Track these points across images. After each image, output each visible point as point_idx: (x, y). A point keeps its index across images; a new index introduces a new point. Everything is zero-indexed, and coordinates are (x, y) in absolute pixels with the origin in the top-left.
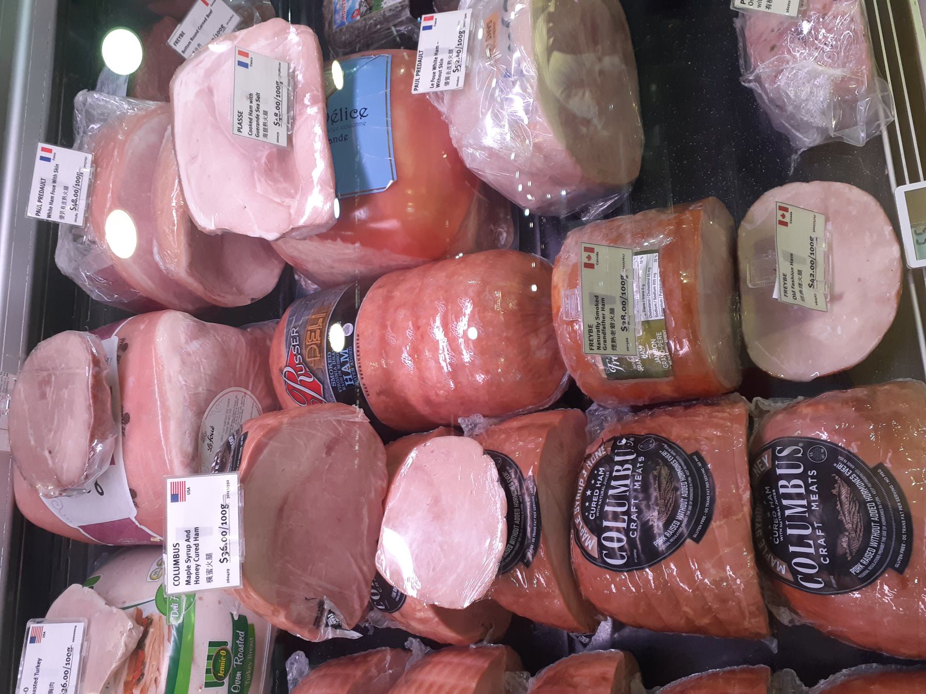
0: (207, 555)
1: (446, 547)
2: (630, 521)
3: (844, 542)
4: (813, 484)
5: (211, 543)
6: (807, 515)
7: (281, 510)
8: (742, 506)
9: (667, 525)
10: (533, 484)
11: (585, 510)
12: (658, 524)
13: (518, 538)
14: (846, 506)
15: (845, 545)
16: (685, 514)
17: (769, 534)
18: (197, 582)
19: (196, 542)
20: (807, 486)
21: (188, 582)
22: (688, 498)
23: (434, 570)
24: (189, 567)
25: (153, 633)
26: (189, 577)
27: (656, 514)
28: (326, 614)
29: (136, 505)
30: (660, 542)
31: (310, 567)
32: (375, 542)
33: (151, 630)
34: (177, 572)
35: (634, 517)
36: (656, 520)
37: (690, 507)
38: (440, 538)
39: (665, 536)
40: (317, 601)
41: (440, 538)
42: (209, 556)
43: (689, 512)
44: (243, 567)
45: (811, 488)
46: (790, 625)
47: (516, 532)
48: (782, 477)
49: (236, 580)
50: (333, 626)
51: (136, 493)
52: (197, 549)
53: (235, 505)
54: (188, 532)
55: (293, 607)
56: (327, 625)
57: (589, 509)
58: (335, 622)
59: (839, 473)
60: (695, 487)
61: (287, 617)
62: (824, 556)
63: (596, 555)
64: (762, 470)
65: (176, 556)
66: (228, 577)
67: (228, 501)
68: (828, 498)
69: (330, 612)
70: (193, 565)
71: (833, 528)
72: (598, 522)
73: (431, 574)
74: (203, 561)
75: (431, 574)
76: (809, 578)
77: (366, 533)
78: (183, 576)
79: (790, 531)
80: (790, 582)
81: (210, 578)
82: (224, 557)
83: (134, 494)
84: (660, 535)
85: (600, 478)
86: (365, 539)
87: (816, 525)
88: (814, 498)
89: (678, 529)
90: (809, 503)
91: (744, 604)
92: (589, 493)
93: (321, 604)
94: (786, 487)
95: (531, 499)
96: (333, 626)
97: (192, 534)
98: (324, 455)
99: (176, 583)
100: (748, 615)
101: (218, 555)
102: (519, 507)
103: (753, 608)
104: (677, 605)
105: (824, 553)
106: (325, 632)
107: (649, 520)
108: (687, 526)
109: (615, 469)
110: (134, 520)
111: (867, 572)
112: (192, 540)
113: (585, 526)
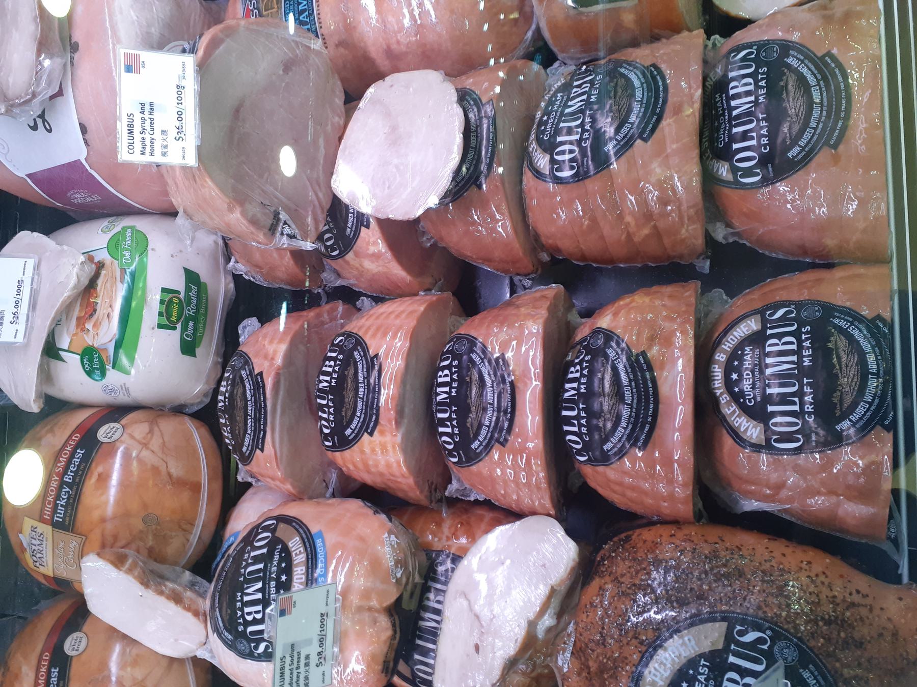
0: (162, 131)
1: (402, 168)
2: (584, 131)
3: (785, 129)
4: (762, 79)
5: (165, 119)
6: (753, 109)
7: (237, 111)
8: (693, 103)
9: (618, 130)
10: (491, 107)
11: (540, 133)
12: (610, 131)
13: (472, 161)
14: (792, 94)
15: (786, 130)
16: (637, 117)
17: (713, 140)
18: (152, 154)
19: (151, 116)
20: (756, 82)
21: (143, 153)
22: (641, 101)
23: (389, 187)
24: (143, 138)
25: (105, 275)
26: (144, 148)
27: (609, 120)
28: (281, 224)
29: (86, 143)
30: (610, 147)
31: (266, 175)
32: (330, 170)
33: (103, 272)
34: (132, 141)
35: (587, 127)
36: (608, 126)
37: (643, 110)
38: (396, 161)
39: (616, 140)
40: (273, 209)
41: (396, 161)
42: (164, 132)
43: (641, 114)
44: (199, 149)
45: (760, 84)
46: (724, 242)
47: (471, 155)
48: (733, 79)
49: (191, 160)
50: (288, 235)
51: (86, 128)
52: (151, 123)
53: (191, 86)
54: (143, 105)
55: (248, 206)
56: (282, 234)
57: (543, 132)
58: (290, 233)
59: (789, 66)
60: (649, 90)
61: (243, 214)
62: (765, 145)
63: (547, 171)
64: (714, 80)
65: (131, 126)
66: (184, 155)
67: (183, 83)
68: (775, 91)
69: (285, 223)
70: (148, 138)
71: (775, 118)
72: (552, 140)
73: (386, 191)
74: (157, 135)
75: (386, 191)
76: (748, 172)
77: (322, 162)
78: (138, 146)
79: (735, 130)
80: (729, 182)
81: (165, 153)
82: (180, 135)
83: (84, 129)
84: (611, 139)
85: (558, 103)
86: (321, 168)
87: (761, 116)
88: (763, 91)
89: (629, 131)
90: (757, 99)
91: (684, 207)
92: (545, 118)
93: (276, 215)
94: (736, 88)
95: (489, 121)
96: (288, 235)
97: (147, 108)
98: (281, 72)
99: (131, 151)
100: (686, 222)
101: (173, 133)
102: (476, 131)
103: (692, 211)
104: (620, 217)
105: (766, 142)
106: (280, 241)
107: (601, 128)
108: (638, 127)
109: (573, 91)
110: (84, 162)
111: (804, 153)
112: (147, 113)
113: (539, 148)
